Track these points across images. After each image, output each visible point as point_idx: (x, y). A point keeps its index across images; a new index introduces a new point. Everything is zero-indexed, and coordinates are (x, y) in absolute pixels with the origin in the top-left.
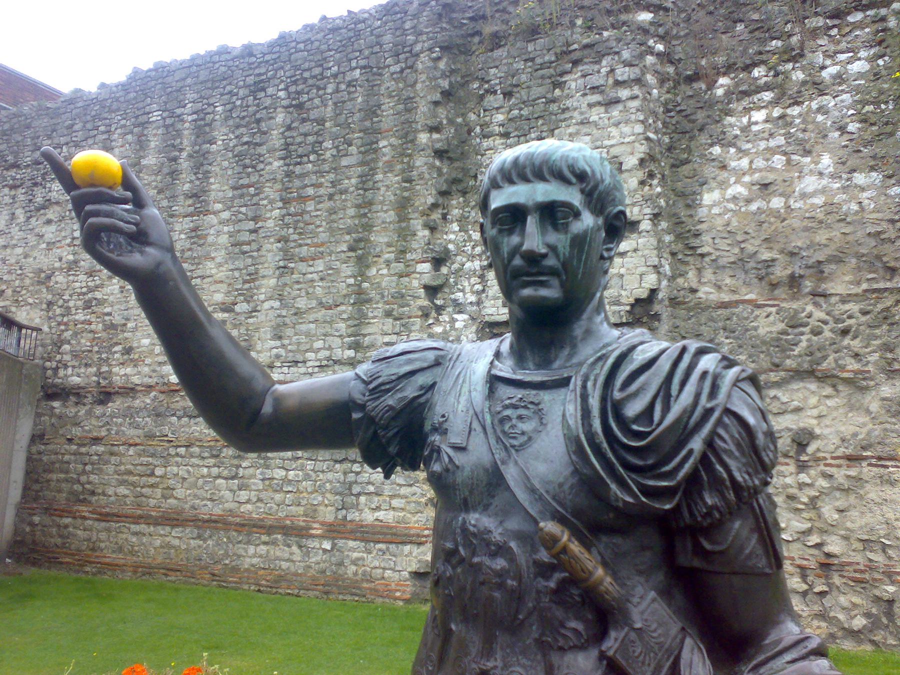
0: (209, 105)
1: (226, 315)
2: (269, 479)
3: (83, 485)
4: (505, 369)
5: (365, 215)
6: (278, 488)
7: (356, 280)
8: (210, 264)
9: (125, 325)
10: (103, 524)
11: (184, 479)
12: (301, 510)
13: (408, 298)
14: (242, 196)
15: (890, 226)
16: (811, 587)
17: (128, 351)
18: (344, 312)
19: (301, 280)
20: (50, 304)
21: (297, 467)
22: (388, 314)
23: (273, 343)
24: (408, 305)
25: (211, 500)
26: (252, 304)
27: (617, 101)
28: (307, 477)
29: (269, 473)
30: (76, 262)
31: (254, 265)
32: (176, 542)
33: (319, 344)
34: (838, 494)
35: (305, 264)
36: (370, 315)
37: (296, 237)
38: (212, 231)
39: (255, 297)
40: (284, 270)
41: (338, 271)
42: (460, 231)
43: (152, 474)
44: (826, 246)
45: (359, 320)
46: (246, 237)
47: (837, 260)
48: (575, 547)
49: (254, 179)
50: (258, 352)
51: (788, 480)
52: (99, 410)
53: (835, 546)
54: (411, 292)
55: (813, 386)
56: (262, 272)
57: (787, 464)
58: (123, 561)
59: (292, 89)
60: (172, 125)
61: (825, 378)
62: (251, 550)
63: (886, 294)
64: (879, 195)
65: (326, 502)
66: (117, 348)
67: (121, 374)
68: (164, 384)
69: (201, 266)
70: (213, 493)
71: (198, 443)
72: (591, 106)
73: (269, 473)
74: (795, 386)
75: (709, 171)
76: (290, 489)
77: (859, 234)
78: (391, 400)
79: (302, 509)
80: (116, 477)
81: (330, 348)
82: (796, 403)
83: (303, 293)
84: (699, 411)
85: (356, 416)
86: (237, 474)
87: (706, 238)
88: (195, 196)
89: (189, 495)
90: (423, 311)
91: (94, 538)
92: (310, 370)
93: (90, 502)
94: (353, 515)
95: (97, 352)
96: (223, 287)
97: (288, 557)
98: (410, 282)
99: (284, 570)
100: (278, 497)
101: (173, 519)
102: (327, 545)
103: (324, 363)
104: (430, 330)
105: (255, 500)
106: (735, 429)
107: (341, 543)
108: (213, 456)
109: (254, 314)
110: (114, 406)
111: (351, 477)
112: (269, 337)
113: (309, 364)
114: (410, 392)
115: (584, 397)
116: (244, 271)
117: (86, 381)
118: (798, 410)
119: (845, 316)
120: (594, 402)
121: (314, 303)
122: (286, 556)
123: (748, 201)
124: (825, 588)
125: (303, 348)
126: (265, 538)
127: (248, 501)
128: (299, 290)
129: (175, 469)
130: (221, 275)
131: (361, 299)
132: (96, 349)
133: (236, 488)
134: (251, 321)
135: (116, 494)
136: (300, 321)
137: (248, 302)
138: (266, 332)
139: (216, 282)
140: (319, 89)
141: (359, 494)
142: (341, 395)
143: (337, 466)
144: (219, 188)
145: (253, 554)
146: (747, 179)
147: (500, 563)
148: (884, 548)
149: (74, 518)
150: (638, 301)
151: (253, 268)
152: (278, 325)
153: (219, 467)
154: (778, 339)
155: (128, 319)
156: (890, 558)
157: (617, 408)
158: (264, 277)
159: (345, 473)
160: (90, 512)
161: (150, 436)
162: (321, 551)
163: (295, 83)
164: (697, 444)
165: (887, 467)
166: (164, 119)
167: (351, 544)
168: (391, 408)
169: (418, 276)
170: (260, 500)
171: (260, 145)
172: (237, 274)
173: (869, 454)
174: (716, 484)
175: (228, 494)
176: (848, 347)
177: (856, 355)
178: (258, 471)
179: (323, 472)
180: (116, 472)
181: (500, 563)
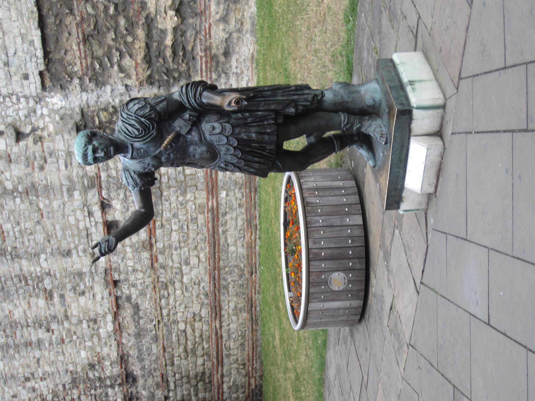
1: (55, 295)
2: (179, 243)
3: (198, 382)
4: (129, 155)
6: (186, 236)
7: (16, 197)
9: (71, 372)
10: (225, 360)
11: (186, 307)
13: (28, 154)
17: (92, 366)
18: (44, 203)
19: (21, 240)
21: (169, 224)
22: (42, 168)
23: (75, 256)
24: (34, 154)
25: (199, 284)
26: (45, 277)
28: (175, 216)
31: (12, 279)
32: (232, 305)
33: (72, 219)
35: (6, 239)
36: (44, 182)
39: (39, 274)
41: (12, 212)
43: (185, 331)
45: (48, 189)
48: (166, 142)
52: (141, 382)
54: (23, 153)
56: (18, 272)
58: (250, 342)
62: (232, 249)
65: (192, 199)
66: (91, 375)
67: (111, 370)
68: (115, 334)
69: (18, 320)
70: (195, 284)
71: (158, 301)
76: (185, 227)
78: (138, 181)
79: (199, 216)
80: (189, 357)
81: (74, 211)
83: (32, 237)
84: (136, 119)
85: (143, 189)
86: (178, 268)
89: (197, 301)
90: (37, 142)
91: (235, 366)
92: (93, 224)
95: (95, 390)
96: (33, 300)
98: (15, 154)
99: (244, 224)
100: (192, 235)
101: (216, 310)
102: (223, 194)
103: (86, 213)
104: (53, 134)
105: (196, 252)
106: (138, 112)
107: (220, 184)
108: (166, 288)
109: (52, 274)
110: (136, 370)
111: (173, 183)
112: (69, 260)
113: (88, 225)
114: (136, 177)
115: (135, 141)
116: (18, 286)
120: (136, 140)
121: (38, 227)
122: (233, 222)
125: (76, 232)
128: (29, 241)
129: (179, 314)
130: (24, 304)
131: (31, 191)
132: (93, 392)
133: (189, 267)
134: (58, 276)
135: (202, 356)
136: (54, 236)
138: (66, 263)
139: (29, 306)
142: (138, 192)
143: (165, 194)
145: (235, 247)
147: (172, 155)
149: (223, 383)
151: (15, 279)
152: (60, 253)
153: (174, 283)
155: (67, 371)
158: (21, 270)
159: (169, 187)
160: (217, 373)
161: (156, 339)
162: (228, 198)
164: (143, 120)
168: (140, 181)
169: (9, 148)
170: (196, 248)
172: (21, 291)
174: (150, 115)
175: (194, 272)
178: (174, 252)
179: (170, 204)
180: (186, 358)
181: (172, 155)
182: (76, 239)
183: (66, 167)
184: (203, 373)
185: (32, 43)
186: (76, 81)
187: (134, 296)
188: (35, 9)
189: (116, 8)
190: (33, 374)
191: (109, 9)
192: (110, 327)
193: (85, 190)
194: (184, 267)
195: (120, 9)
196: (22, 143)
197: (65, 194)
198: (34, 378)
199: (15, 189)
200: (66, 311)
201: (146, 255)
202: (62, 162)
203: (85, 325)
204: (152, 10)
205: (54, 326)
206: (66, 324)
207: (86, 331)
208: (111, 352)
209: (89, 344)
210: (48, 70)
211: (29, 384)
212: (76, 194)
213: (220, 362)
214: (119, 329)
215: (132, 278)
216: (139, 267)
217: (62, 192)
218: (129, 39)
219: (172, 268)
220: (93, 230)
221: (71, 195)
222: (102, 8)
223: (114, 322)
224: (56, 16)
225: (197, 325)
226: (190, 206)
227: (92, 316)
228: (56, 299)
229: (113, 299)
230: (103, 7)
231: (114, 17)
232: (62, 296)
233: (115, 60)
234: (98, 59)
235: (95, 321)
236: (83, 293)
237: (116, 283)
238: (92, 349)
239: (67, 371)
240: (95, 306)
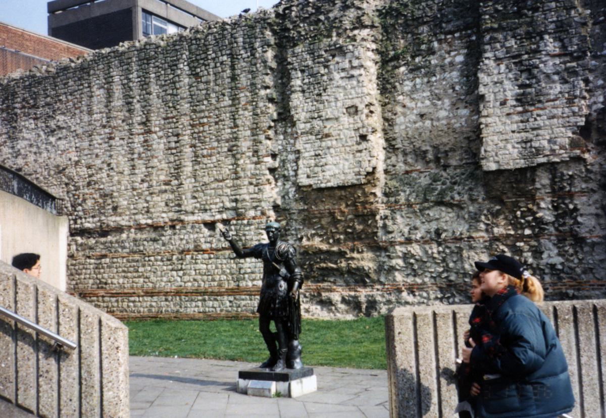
0: (146, 73)
5: (235, 132)
8: (156, 160)
12: (216, 284)
14: (169, 123)
20: (67, 184)
22: (251, 184)
27: (352, 76)
29: (198, 267)
30: (79, 161)
33: (218, 200)
34: (454, 255)
37: (200, 145)
38: (154, 142)
40: (196, 162)
42: (284, 139)
45: (237, 187)
46: (173, 145)
47: (453, 150)
49: (175, 113)
50: (186, 206)
53: (453, 278)
55: (443, 209)
59: (192, 65)
60: (127, 84)
61: (450, 205)
67: (112, 220)
68: (138, 225)
72: (342, 78)
73: (198, 267)
74: (435, 208)
75: (399, 109)
77: (461, 138)
82: (437, 216)
83: (206, 174)
87: (399, 140)
88: (144, 124)
93: (105, 288)
94: (243, 284)
97: (213, 306)
107: (237, 297)
113: (213, 211)
117: (94, 225)
118: (437, 219)
123: (415, 123)
126: (200, 298)
127: (189, 281)
135: (119, 283)
137: (178, 180)
140: (205, 65)
141: (244, 274)
143: (232, 261)
144: (156, 121)
145: (193, 308)
146: (415, 111)
154: (428, 188)
163: (192, 61)
166: (121, 80)
167: (243, 297)
171: (176, 95)
175: (179, 279)
182: (204, 203)
183: (252, 199)
184: (106, 284)
185: (329, 181)
186: (306, 207)
187: (163, 238)
188: (350, 184)
190: (112, 169)
192: (143, 222)
193: (235, 209)
194: (182, 272)
195: (350, 236)
196: (267, 172)
197: (234, 197)
198: (109, 170)
199: (238, 165)
200: (155, 193)
201: (191, 246)
202: (255, 196)
203: (145, 205)
205: (146, 185)
206: (147, 193)
207: (140, 206)
208: (123, 221)
209: (132, 207)
210: (313, 190)
211: (105, 166)
212: (234, 204)
213: (113, 295)
214: (140, 228)
215: (176, 237)
216: (184, 242)
217: (235, 195)
218: (331, 241)
219: (182, 264)
220: (209, 213)
221: (233, 201)
223: (146, 224)
224: (345, 196)
225: (142, 280)
226: (224, 277)
227: (152, 210)
228: (164, 187)
229: (162, 224)
231: (346, 233)
232: (165, 191)
233: (319, 232)
234: (320, 221)
235: (148, 212)
236: (167, 205)
237: (173, 227)
238: (129, 209)
239: (113, 191)
240: (158, 212)
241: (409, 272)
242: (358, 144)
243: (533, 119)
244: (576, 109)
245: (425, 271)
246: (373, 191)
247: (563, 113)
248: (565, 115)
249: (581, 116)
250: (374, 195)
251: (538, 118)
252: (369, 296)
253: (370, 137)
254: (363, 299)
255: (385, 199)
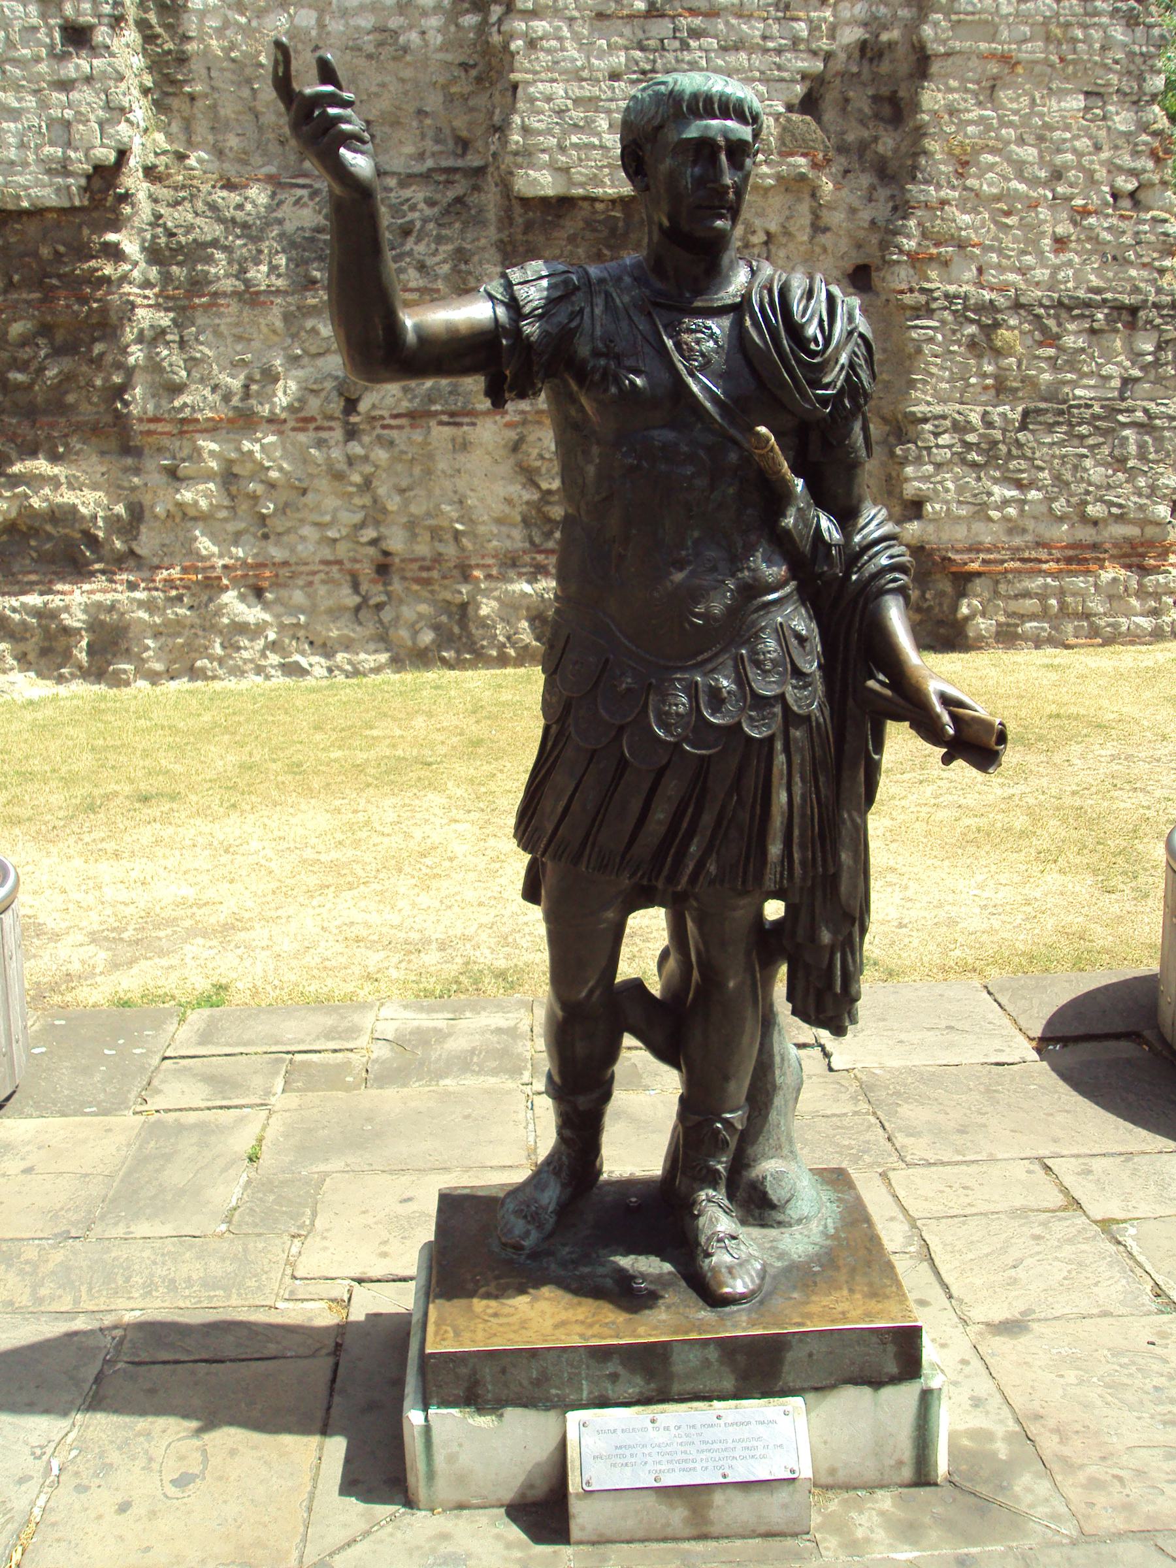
15: (463, 74)
16: (365, 599)
34: (399, 467)
44: (377, 95)
51: (336, 454)
53: (396, 543)
57: (331, 429)
63: (457, 177)
64: (446, 25)
84: (845, 334)
119: (405, 207)
124: (384, 598)
148: (457, 535)
150: (99, 169)
154: (312, 240)
156: (463, 549)
157: (795, 331)
165: (458, 424)
173: (438, 407)
176: (410, 253)
177: (422, 267)
189: (19, 386)
191: (19, 370)
204: (17, 468)
222: (26, 353)
230: (26, 357)
241: (242, 525)
242: (63, 57)
243: (677, 44)
244: (802, 28)
245: (302, 521)
246: (111, 237)
247: (764, 38)
248: (771, 45)
249: (815, 53)
250: (115, 253)
251: (693, 44)
252: (99, 605)
253: (101, 34)
254: (75, 619)
255: (154, 273)
